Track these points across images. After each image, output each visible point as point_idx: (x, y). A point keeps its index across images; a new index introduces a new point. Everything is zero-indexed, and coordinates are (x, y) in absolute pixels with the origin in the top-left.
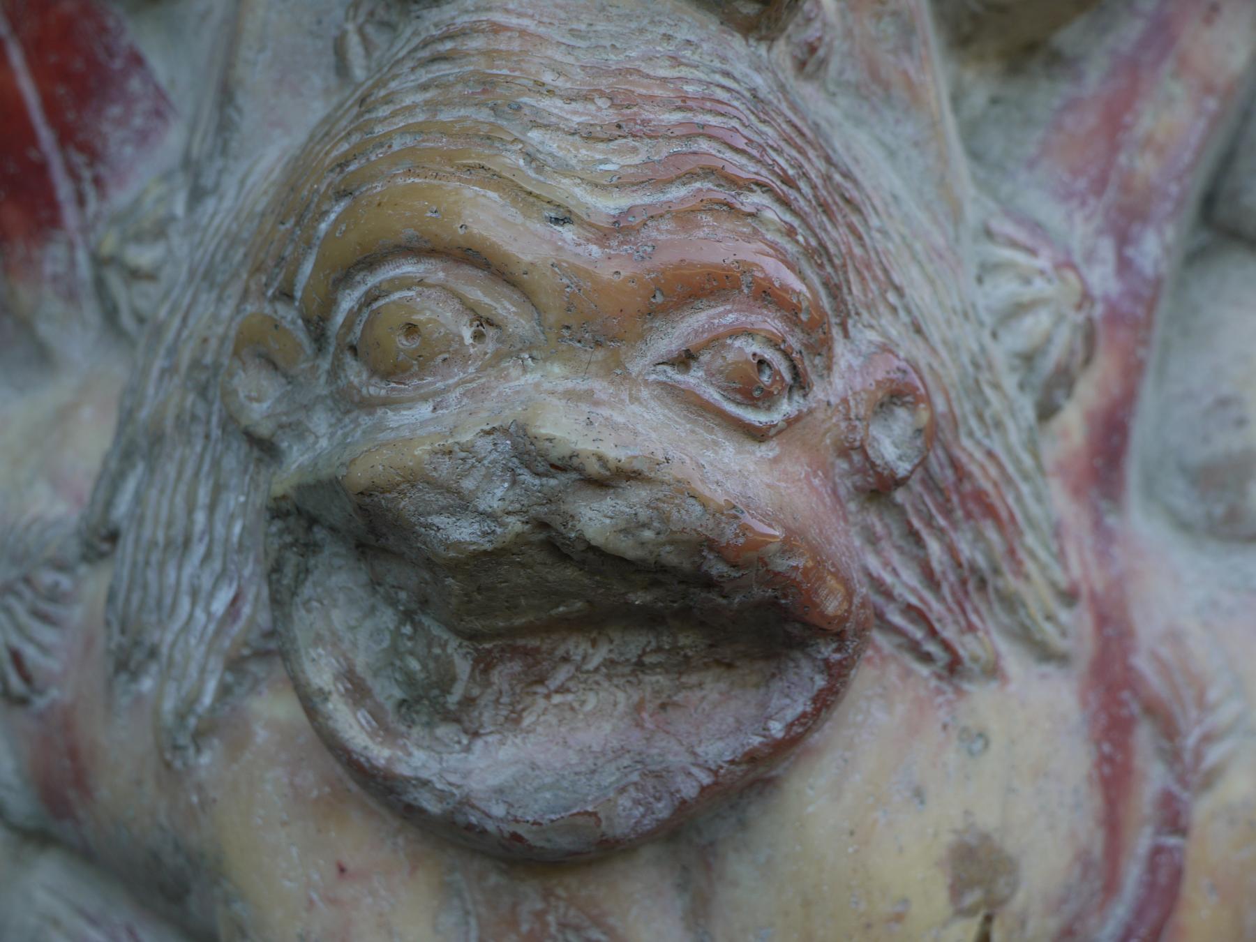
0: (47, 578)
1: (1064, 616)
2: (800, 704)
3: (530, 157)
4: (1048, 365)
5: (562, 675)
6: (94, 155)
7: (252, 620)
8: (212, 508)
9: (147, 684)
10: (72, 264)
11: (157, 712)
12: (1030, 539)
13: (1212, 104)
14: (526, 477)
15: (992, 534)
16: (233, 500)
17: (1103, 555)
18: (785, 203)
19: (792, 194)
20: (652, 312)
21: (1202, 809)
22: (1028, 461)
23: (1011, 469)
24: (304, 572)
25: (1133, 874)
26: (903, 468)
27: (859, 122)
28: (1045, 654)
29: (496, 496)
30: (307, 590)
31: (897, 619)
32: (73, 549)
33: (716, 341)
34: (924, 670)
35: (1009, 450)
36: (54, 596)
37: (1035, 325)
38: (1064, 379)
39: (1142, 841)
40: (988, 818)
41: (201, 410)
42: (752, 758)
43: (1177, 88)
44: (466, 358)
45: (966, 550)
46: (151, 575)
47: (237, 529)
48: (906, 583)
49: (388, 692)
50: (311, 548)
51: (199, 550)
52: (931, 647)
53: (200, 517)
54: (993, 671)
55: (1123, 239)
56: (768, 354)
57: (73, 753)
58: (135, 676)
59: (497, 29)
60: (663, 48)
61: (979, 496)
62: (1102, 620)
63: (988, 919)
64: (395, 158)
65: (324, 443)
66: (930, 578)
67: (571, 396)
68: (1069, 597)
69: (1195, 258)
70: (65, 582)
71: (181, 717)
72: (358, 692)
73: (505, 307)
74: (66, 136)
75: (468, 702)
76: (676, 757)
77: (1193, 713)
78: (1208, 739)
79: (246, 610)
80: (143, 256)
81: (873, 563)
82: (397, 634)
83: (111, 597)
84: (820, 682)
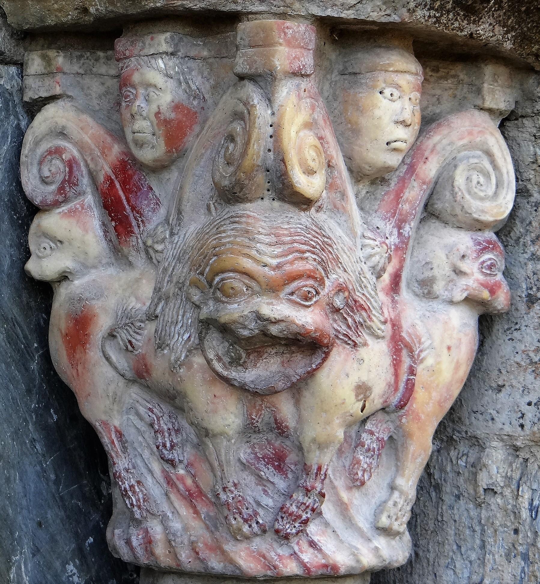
0: (138, 324)
1: (383, 327)
2: (319, 361)
3: (257, 251)
4: (379, 268)
5: (265, 355)
6: (141, 215)
7: (194, 342)
9: (166, 351)
10: (138, 243)
11: (170, 360)
12: (374, 312)
14: (259, 321)
15: (364, 314)
16: (188, 315)
18: (314, 253)
19: (315, 250)
20: (285, 285)
21: (420, 369)
22: (373, 293)
23: (368, 296)
25: (402, 386)
26: (341, 306)
27: (331, 218)
28: (378, 337)
30: (207, 337)
31: (341, 337)
32: (144, 318)
33: (299, 289)
34: (348, 347)
35: (368, 292)
36: (140, 328)
38: (384, 270)
39: (404, 377)
40: (364, 378)
41: (179, 292)
42: (308, 373)
43: (415, 184)
45: (357, 318)
46: (167, 328)
47: (190, 321)
48: (343, 328)
49: (226, 360)
50: (208, 329)
52: (349, 342)
53: (180, 317)
54: (365, 344)
55: (399, 228)
56: (310, 289)
57: (146, 365)
58: (163, 350)
59: (249, 216)
60: (286, 219)
61: (361, 306)
62: (394, 325)
63: (365, 401)
64: (228, 250)
65: (212, 308)
66: (349, 327)
67: (268, 304)
68: (385, 322)
70: (143, 325)
72: (219, 359)
73: (254, 284)
74: (133, 208)
75: (245, 362)
76: (292, 372)
77: (417, 345)
78: (421, 351)
79: (192, 339)
80: (159, 247)
81: (335, 326)
82: (229, 348)
83: (156, 331)
84: (324, 356)
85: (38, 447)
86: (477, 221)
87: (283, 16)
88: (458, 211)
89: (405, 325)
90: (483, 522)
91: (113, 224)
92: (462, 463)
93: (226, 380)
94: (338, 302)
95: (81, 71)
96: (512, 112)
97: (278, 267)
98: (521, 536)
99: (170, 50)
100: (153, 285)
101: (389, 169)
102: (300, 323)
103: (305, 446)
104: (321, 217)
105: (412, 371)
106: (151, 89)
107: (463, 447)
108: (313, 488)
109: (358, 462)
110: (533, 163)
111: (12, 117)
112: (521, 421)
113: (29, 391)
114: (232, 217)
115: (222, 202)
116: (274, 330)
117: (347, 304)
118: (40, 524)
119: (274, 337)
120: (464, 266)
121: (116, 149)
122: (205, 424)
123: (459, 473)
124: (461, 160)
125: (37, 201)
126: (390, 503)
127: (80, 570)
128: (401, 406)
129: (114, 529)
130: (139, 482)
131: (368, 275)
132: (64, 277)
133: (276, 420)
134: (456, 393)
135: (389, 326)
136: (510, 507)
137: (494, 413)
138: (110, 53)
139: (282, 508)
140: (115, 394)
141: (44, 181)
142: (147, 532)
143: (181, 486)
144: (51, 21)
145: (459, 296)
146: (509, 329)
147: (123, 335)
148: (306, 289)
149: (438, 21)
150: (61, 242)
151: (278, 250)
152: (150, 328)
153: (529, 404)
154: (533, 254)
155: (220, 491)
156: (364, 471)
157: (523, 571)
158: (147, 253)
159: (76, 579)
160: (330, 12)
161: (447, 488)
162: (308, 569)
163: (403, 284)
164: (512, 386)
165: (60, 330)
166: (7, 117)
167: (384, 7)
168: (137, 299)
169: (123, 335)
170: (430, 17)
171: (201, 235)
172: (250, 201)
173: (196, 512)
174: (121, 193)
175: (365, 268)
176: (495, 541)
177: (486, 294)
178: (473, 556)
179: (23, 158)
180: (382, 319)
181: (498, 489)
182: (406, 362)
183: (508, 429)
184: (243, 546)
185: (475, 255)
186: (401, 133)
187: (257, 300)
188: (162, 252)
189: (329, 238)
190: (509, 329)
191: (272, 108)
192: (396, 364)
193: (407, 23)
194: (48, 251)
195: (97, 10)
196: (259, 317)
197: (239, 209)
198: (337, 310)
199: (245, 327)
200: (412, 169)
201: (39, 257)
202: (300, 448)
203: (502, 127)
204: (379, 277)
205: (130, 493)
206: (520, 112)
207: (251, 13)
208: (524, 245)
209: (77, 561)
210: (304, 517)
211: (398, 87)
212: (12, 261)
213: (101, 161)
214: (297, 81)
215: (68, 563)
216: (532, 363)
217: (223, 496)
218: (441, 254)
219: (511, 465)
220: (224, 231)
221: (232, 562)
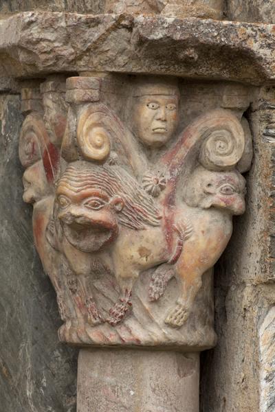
13: (188, 150)
21: (186, 244)
28: (154, 226)
29: (69, 219)
33: (89, 201)
55: (171, 171)
62: (167, 220)
68: (160, 218)
78: (187, 233)
85: (35, 288)
86: (219, 167)
93: (75, 246)
94: (118, 207)
97: (78, 191)
102: (90, 217)
104: (116, 167)
116: (78, 221)
119: (80, 224)
120: (210, 190)
128: (174, 261)
131: (146, 195)
135: (163, 220)
140: (52, 258)
162: (123, 341)
163: (178, 200)
175: (144, 193)
182: (177, 240)
184: (94, 329)
186: (158, 124)
187: (72, 206)
192: (169, 241)
198: (118, 212)
210: (120, 314)
211: (157, 102)
218: (199, 184)
221: (89, 338)
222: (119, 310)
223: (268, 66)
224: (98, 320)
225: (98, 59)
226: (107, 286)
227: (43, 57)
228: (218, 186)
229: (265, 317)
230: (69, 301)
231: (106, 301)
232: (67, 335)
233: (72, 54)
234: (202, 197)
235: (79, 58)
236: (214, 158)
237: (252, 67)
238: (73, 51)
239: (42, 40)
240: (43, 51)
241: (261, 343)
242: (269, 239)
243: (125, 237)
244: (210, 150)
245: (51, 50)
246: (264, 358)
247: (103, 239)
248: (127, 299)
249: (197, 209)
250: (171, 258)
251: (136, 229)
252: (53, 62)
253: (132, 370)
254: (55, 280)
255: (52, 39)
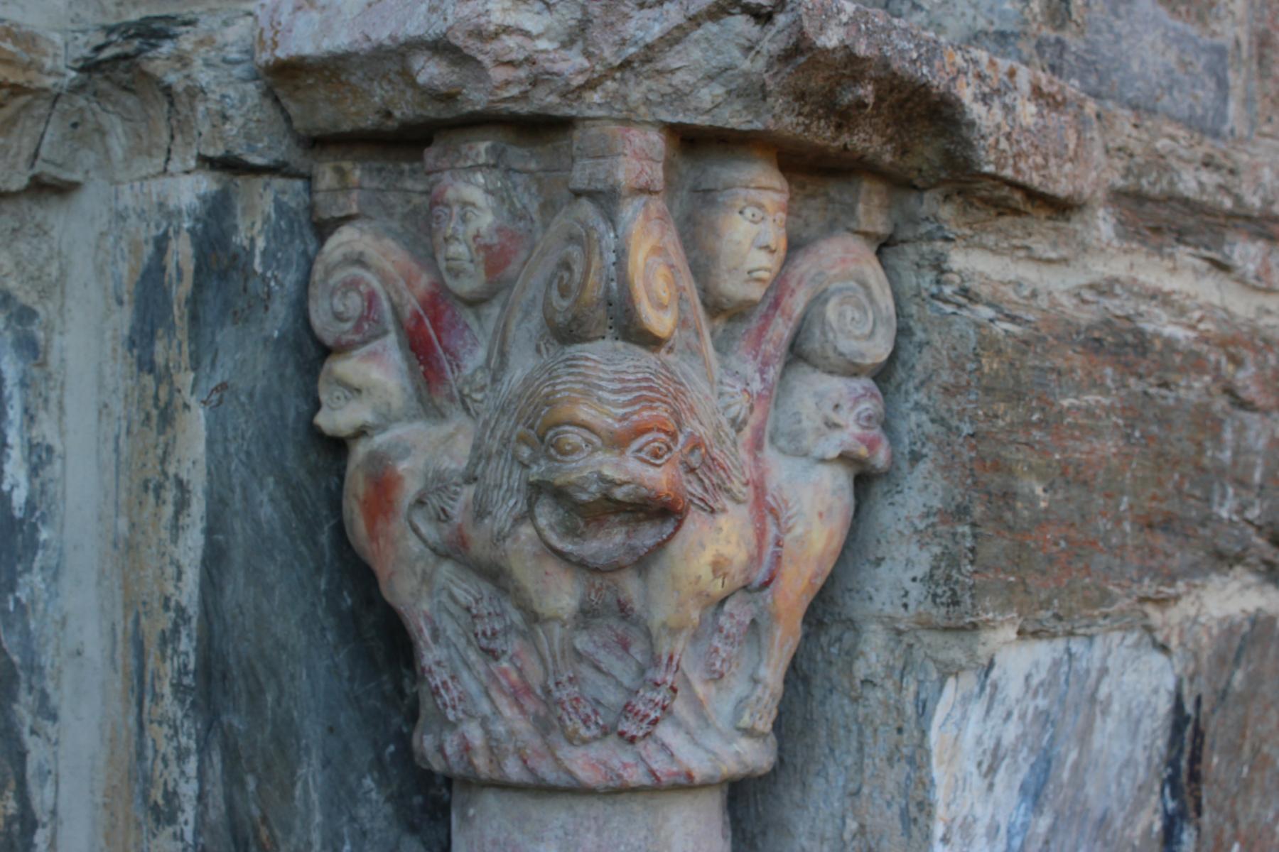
0: (453, 488)
1: (744, 490)
8: (509, 477)
12: (735, 472)
15: (722, 473)
17: (757, 467)
18: (665, 402)
21: (787, 539)
24: (537, 499)
25: (767, 558)
28: (738, 502)
29: (594, 488)
32: (460, 480)
33: (648, 443)
34: (703, 513)
36: (456, 493)
37: (733, 411)
38: (745, 422)
39: (769, 549)
44: (582, 450)
45: (715, 480)
48: (698, 491)
51: (505, 487)
53: (505, 480)
55: (762, 372)
57: (462, 537)
59: (587, 359)
62: (756, 488)
66: (706, 490)
68: (746, 484)
69: (788, 365)
71: (499, 533)
72: (552, 528)
73: (595, 439)
74: (446, 350)
78: (790, 518)
80: (479, 396)
83: (475, 496)
86: (854, 364)
87: (626, 122)
88: (830, 353)
89: (771, 484)
90: (860, 720)
91: (422, 368)
92: (834, 650)
94: (695, 460)
95: (382, 186)
96: (891, 236)
97: (624, 418)
98: (905, 735)
99: (492, 162)
100: (470, 441)
101: (752, 304)
103: (654, 631)
104: (671, 358)
105: (778, 543)
106: (469, 208)
107: (835, 631)
108: (665, 682)
109: (716, 650)
110: (916, 296)
111: (297, 241)
112: (905, 600)
113: (318, 570)
114: (568, 359)
115: (555, 342)
116: (619, 494)
117: (703, 462)
118: (331, 730)
119: (618, 502)
120: (835, 418)
121: (424, 282)
122: (536, 607)
123: (830, 663)
124: (833, 293)
125: (329, 340)
126: (754, 698)
127: (379, 783)
128: (766, 585)
129: (422, 734)
130: (453, 678)
131: (727, 428)
132: (362, 432)
133: (619, 601)
134: (829, 567)
135: (751, 487)
136: (892, 702)
137: (872, 591)
138: (417, 165)
139: (626, 706)
140: (424, 572)
141: (339, 317)
142: (464, 737)
143: (504, 682)
144: (346, 127)
145: (833, 453)
146: (889, 491)
147: (435, 501)
148: (656, 444)
149: (807, 128)
150: (359, 391)
151: (623, 398)
152: (468, 492)
153: (914, 580)
154: (917, 403)
155: (552, 686)
156: (723, 661)
157: (908, 777)
158: (463, 402)
159: (374, 795)
160: (681, 118)
161: (817, 680)
162: (658, 779)
164: (893, 559)
165: (356, 496)
166: (292, 241)
167: (744, 113)
168: (452, 457)
169: (434, 501)
170: (798, 124)
171: (527, 382)
172: (589, 340)
173: (523, 711)
174: (432, 332)
175: (724, 421)
176: (875, 743)
177: (863, 451)
178: (850, 761)
179: (312, 290)
180: (744, 480)
181: (877, 681)
182: (772, 531)
183: (888, 609)
184: (580, 751)
185: (850, 404)
187: (599, 456)
188: (481, 402)
189: (681, 384)
190: (889, 491)
191: (615, 230)
192: (761, 534)
193: (770, 132)
194: (342, 402)
195: (403, 114)
196: (602, 478)
197: (574, 350)
198: (692, 470)
199: (584, 490)
200: (776, 304)
201: (333, 409)
202: (648, 634)
203: (879, 253)
204: (739, 430)
205: (443, 692)
206: (900, 236)
207: (589, 119)
208: (907, 392)
209: (376, 775)
210: (653, 716)
211: (760, 206)
212: (299, 414)
213: (407, 294)
214: (645, 198)
215: (364, 776)
216: (916, 531)
217: (557, 694)
218: (810, 402)
219: (892, 651)
220: (558, 377)
222: (651, 705)
223: (982, 142)
224: (595, 731)
225: (643, 88)
226: (605, 646)
227: (499, 74)
228: (852, 409)
229: (936, 702)
230: (465, 675)
231: (600, 680)
232: (481, 762)
233: (581, 72)
234: (819, 434)
235: (591, 85)
236: (846, 345)
237: (942, 142)
238: (587, 64)
239: (507, 30)
240: (506, 59)
241: (934, 761)
242: (967, 529)
243: (695, 524)
244: (835, 325)
245: (526, 59)
246: (940, 795)
247: (648, 535)
248: (670, 678)
249: (803, 462)
250: (759, 576)
251: (713, 511)
252: (523, 88)
253: (646, 838)
254: (422, 623)
255: (535, 32)
